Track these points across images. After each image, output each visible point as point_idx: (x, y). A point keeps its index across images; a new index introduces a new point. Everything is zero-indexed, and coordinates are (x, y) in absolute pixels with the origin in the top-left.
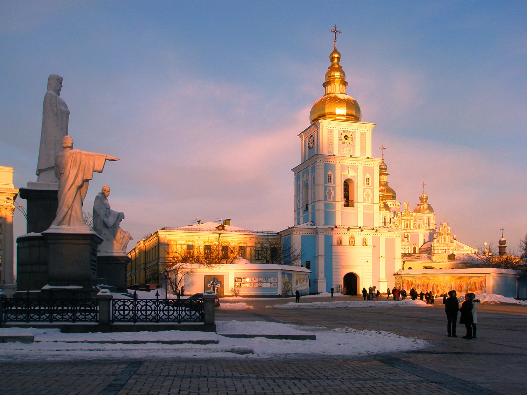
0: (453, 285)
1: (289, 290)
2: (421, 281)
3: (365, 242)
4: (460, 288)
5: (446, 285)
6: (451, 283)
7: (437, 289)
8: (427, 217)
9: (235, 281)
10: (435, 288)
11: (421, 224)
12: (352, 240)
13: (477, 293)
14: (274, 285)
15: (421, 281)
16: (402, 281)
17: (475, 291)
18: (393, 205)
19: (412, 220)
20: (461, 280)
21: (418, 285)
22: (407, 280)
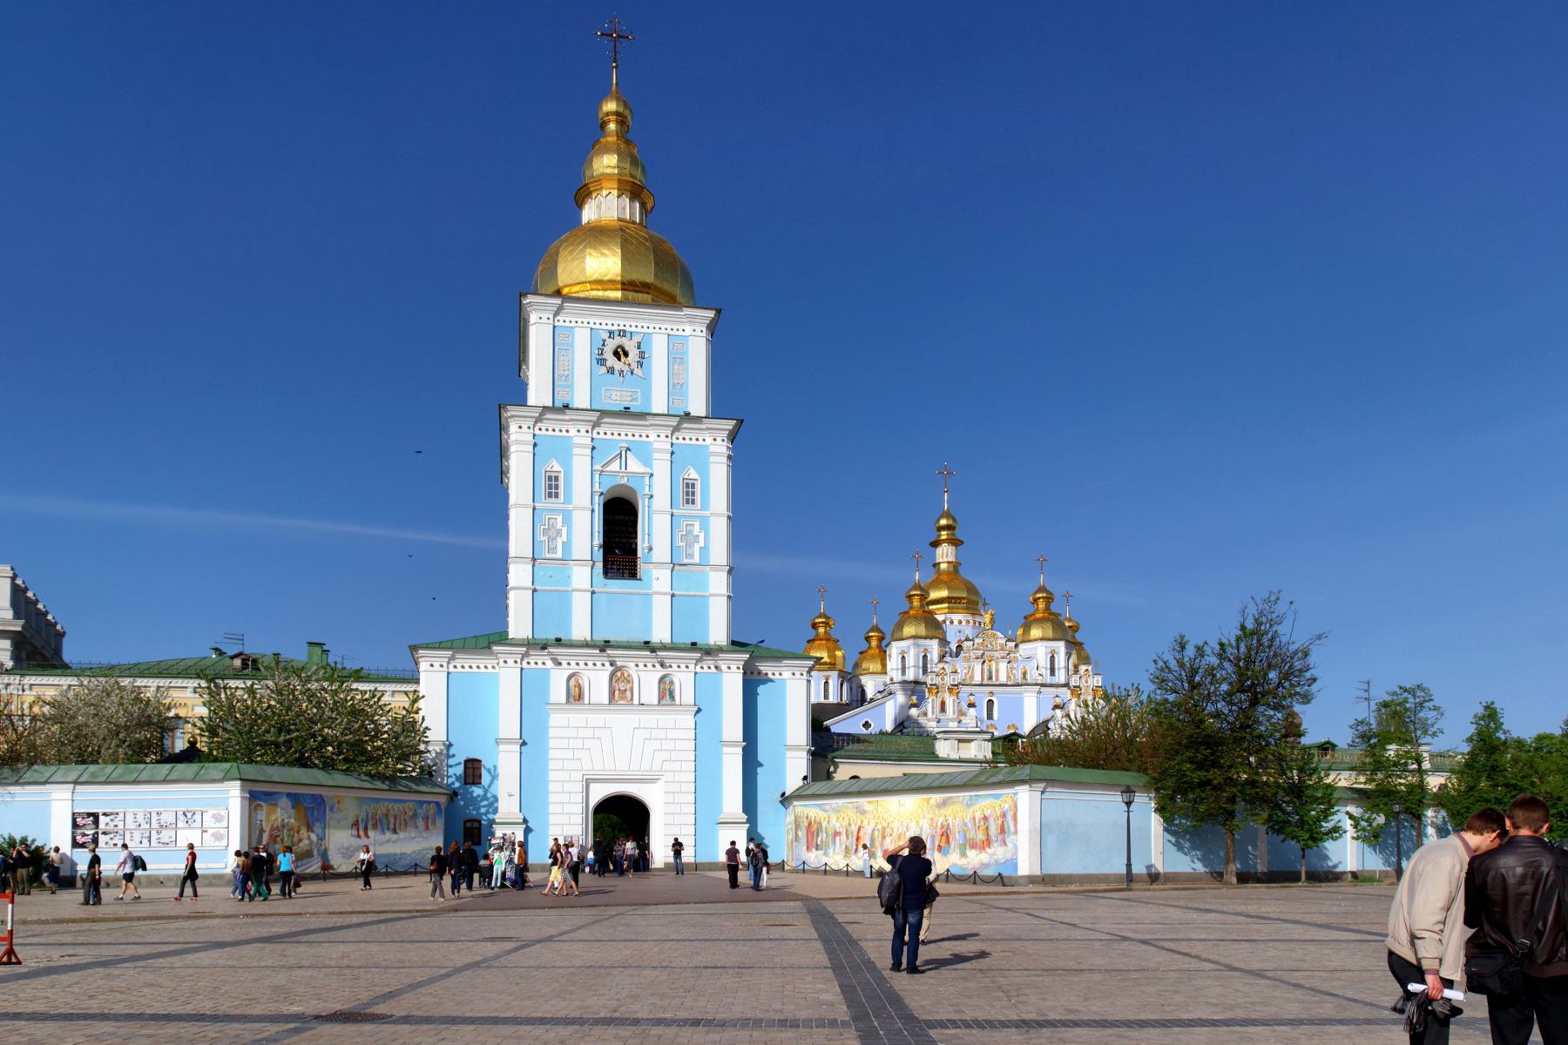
1: (308, 854)
3: (666, 692)
4: (944, 837)
5: (907, 830)
7: (882, 846)
9: (75, 825)
11: (1031, 671)
12: (622, 686)
14: (218, 837)
15: (841, 819)
16: (796, 820)
17: (987, 850)
18: (968, 622)
19: (1002, 658)
20: (949, 811)
21: (836, 834)
22: (807, 818)
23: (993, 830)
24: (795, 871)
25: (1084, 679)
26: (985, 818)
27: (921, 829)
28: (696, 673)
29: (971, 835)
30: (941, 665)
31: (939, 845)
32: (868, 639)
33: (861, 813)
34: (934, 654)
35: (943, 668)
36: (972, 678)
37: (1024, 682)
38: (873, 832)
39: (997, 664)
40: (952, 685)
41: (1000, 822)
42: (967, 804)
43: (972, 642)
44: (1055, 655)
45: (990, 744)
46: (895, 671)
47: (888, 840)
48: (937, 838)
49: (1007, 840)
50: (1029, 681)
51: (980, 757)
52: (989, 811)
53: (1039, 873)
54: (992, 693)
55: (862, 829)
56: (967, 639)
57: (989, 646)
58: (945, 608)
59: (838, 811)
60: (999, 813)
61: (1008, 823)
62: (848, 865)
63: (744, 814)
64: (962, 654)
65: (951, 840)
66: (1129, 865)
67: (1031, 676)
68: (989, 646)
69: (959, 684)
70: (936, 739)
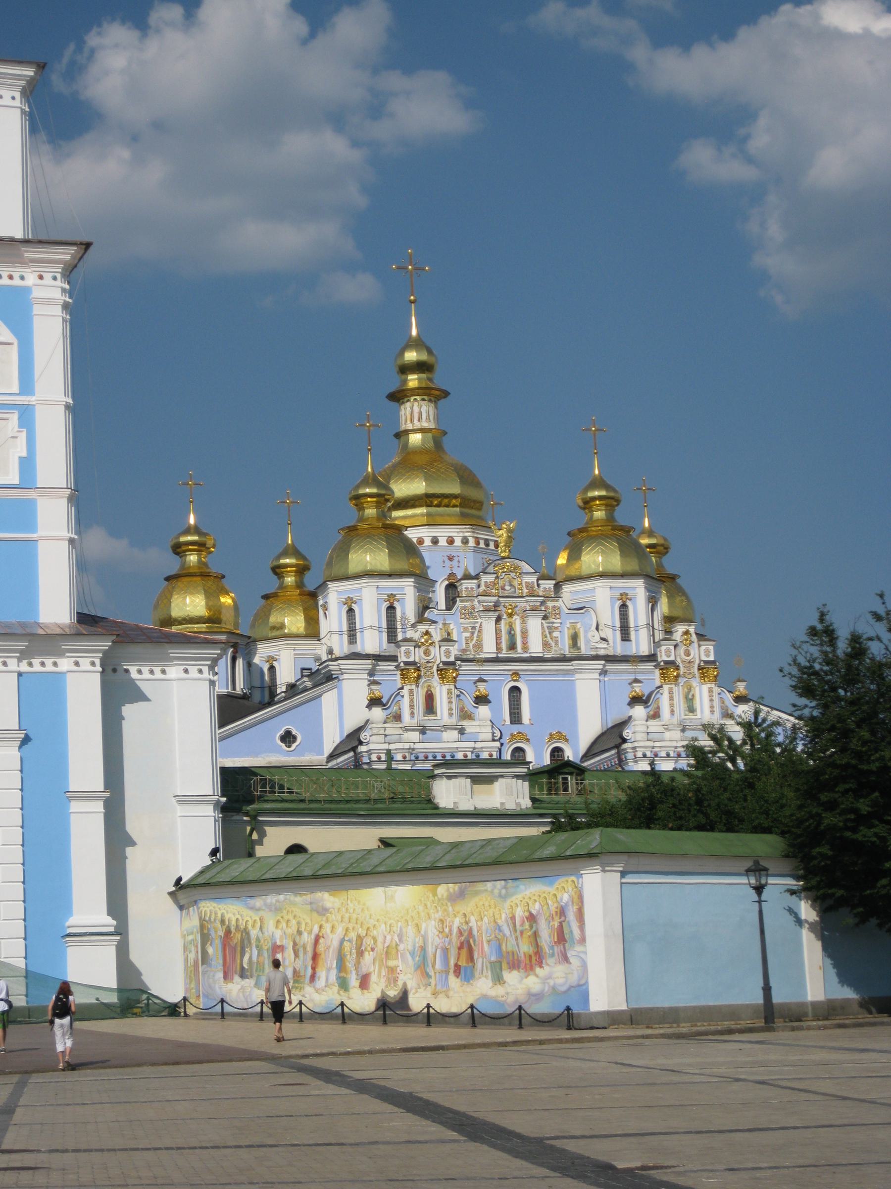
0: (430, 941)
2: (283, 924)
4: (464, 952)
5: (400, 940)
6: (424, 926)
7: (357, 965)
8: (617, 594)
10: (350, 965)
11: (586, 632)
13: (545, 980)
15: (284, 925)
16: (202, 927)
17: (538, 970)
18: (465, 541)
20: (469, 906)
22: (222, 922)
23: (546, 937)
24: (205, 1015)
25: (682, 650)
26: (532, 918)
27: (425, 938)
28: (20, 674)
29: (509, 945)
30: (422, 628)
31: (456, 965)
32: (278, 571)
33: (318, 912)
34: (408, 608)
35: (427, 633)
36: (479, 646)
37: (575, 653)
38: (342, 942)
39: (523, 622)
40: (445, 663)
41: (556, 924)
42: (500, 896)
43: (475, 581)
44: (629, 603)
45: (526, 784)
46: (335, 638)
47: (368, 957)
48: (453, 953)
49: (569, 955)
50: (584, 651)
51: (511, 806)
52: (537, 906)
53: (624, 1007)
54: (516, 675)
55: (321, 941)
56: (467, 577)
57: (507, 588)
58: (422, 515)
59: (277, 910)
60: (553, 909)
61: (570, 926)
62: (301, 1003)
63: (110, 918)
64: (459, 604)
65: (476, 956)
66: (767, 990)
67: (588, 641)
68: (507, 588)
69: (457, 659)
70: (433, 777)
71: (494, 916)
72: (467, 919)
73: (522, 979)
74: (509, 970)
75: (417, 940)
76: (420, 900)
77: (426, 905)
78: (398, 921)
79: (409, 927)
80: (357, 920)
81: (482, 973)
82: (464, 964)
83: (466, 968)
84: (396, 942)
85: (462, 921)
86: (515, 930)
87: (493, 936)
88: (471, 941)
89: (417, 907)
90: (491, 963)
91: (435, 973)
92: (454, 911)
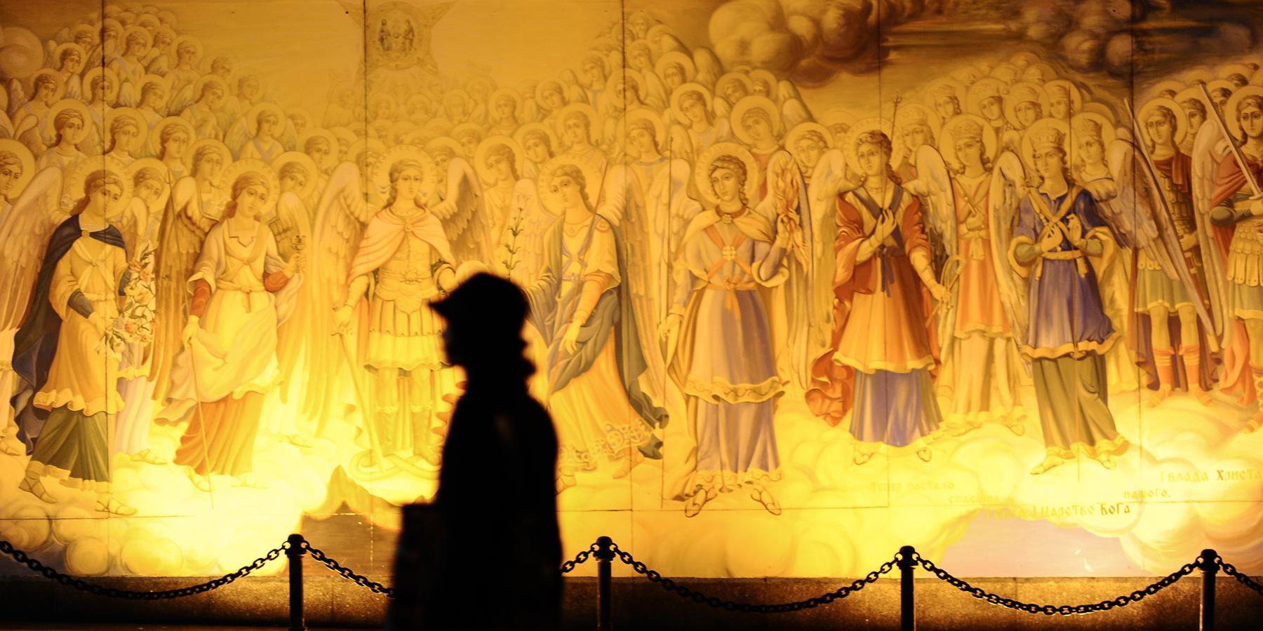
0: (656, 251)
31: (824, 365)
42: (1099, 63)
71: (1060, 150)
72: (895, 163)
73: (1227, 432)
74: (1147, 393)
75: (573, 244)
76: (599, 63)
77: (631, 89)
78: (451, 154)
79: (524, 185)
80: (164, 141)
81: (985, 405)
82: (876, 362)
83: (884, 380)
84: (432, 248)
85: (858, 168)
86: (1191, 225)
87: (1051, 242)
88: (920, 260)
89: (572, 93)
90: (1040, 360)
91: (687, 398)
92: (811, 118)
